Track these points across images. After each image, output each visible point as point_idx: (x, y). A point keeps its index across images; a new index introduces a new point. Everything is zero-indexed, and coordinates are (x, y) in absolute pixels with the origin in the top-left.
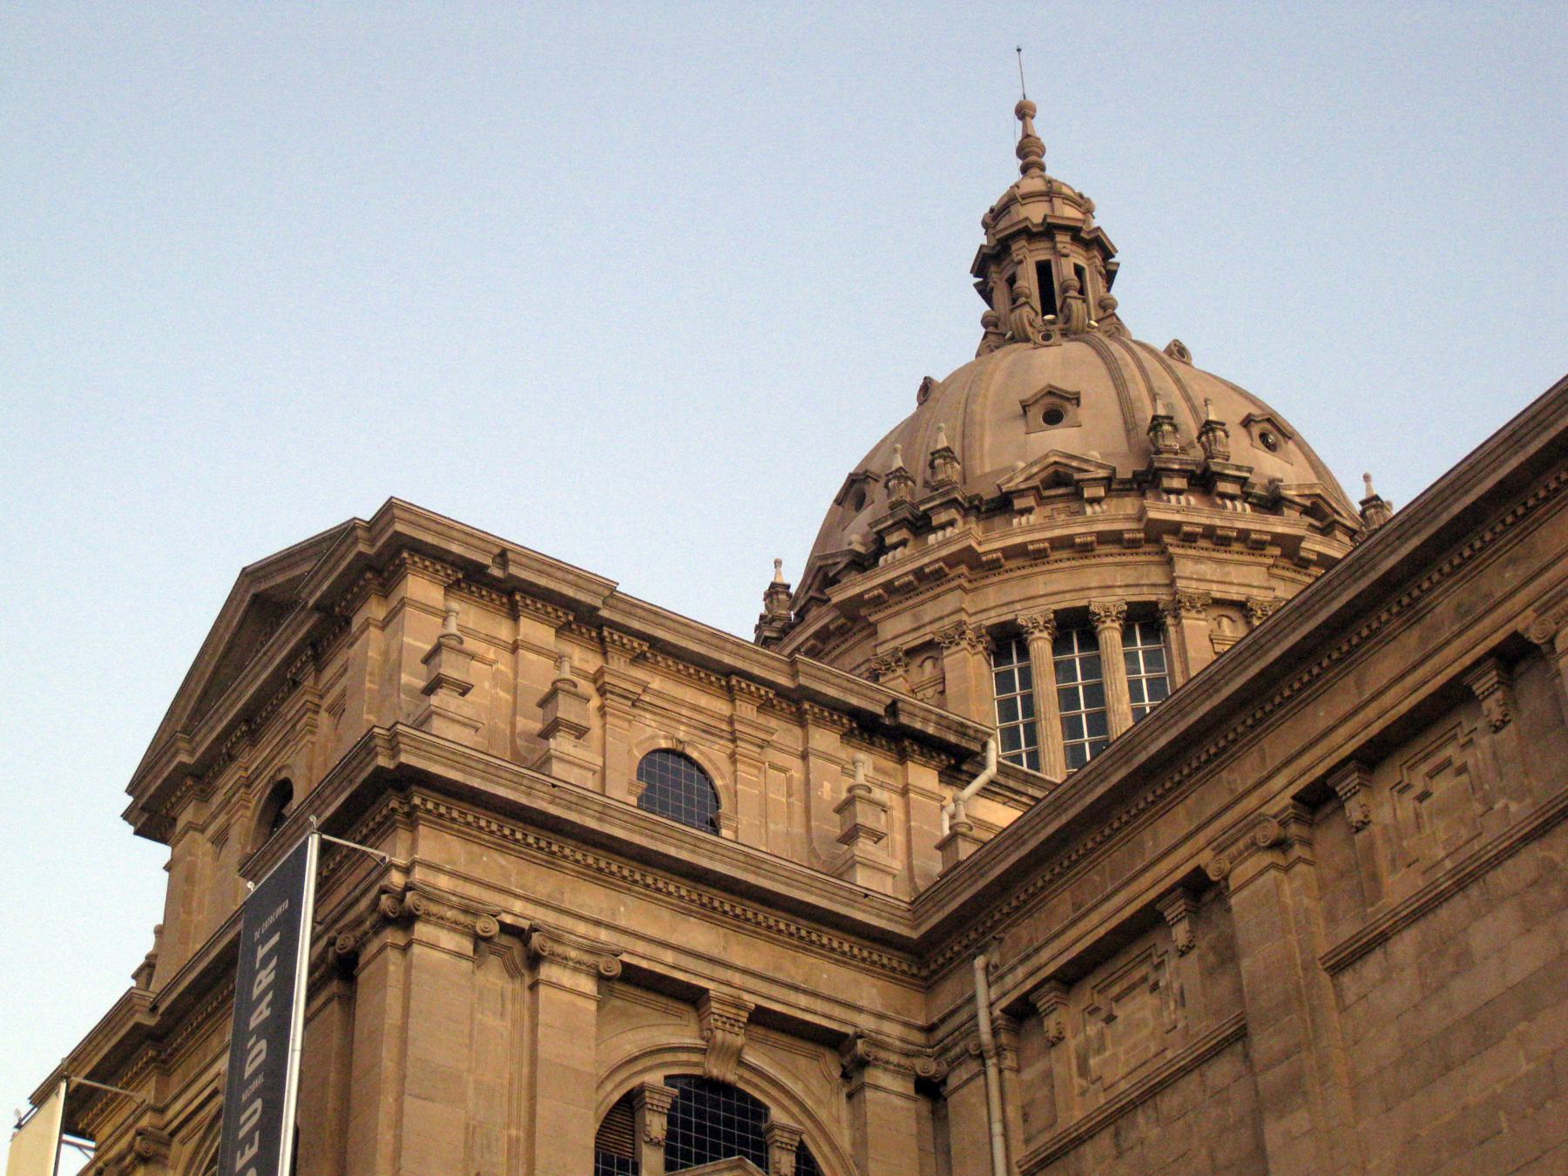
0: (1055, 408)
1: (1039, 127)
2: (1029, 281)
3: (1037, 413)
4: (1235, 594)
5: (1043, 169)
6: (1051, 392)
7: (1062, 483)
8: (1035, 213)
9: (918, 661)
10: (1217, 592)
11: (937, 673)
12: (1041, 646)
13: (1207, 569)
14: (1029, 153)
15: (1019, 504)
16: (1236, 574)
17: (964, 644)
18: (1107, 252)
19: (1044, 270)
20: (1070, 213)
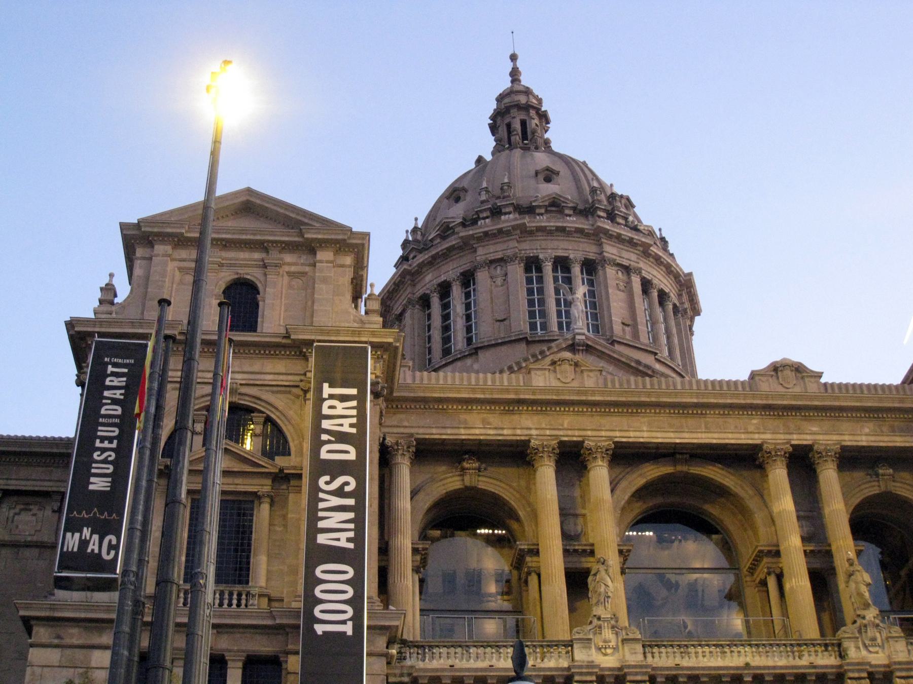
0: (549, 176)
1: (519, 64)
2: (517, 126)
3: (541, 177)
4: (626, 263)
5: (520, 81)
6: (548, 169)
7: (555, 205)
9: (494, 266)
10: (619, 260)
11: (503, 272)
12: (548, 268)
13: (614, 251)
14: (515, 74)
15: (538, 211)
16: (625, 254)
17: (517, 262)
18: (548, 122)
19: (524, 123)
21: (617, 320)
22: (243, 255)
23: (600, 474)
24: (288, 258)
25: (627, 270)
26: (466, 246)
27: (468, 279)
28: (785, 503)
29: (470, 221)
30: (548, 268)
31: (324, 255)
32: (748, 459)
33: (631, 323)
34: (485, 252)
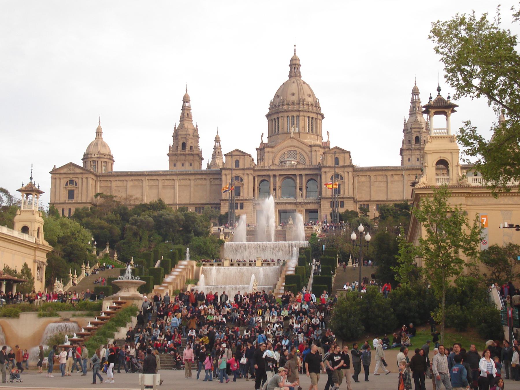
7: (293, 103)
8: (294, 62)
12: (290, 118)
20: (298, 62)
21: (301, 128)
22: (237, 157)
23: (277, 178)
24: (242, 157)
25: (304, 116)
26: (277, 113)
27: (278, 118)
28: (298, 181)
29: (279, 106)
30: (290, 118)
31: (246, 156)
32: (295, 175)
33: (304, 128)
34: (281, 115)
